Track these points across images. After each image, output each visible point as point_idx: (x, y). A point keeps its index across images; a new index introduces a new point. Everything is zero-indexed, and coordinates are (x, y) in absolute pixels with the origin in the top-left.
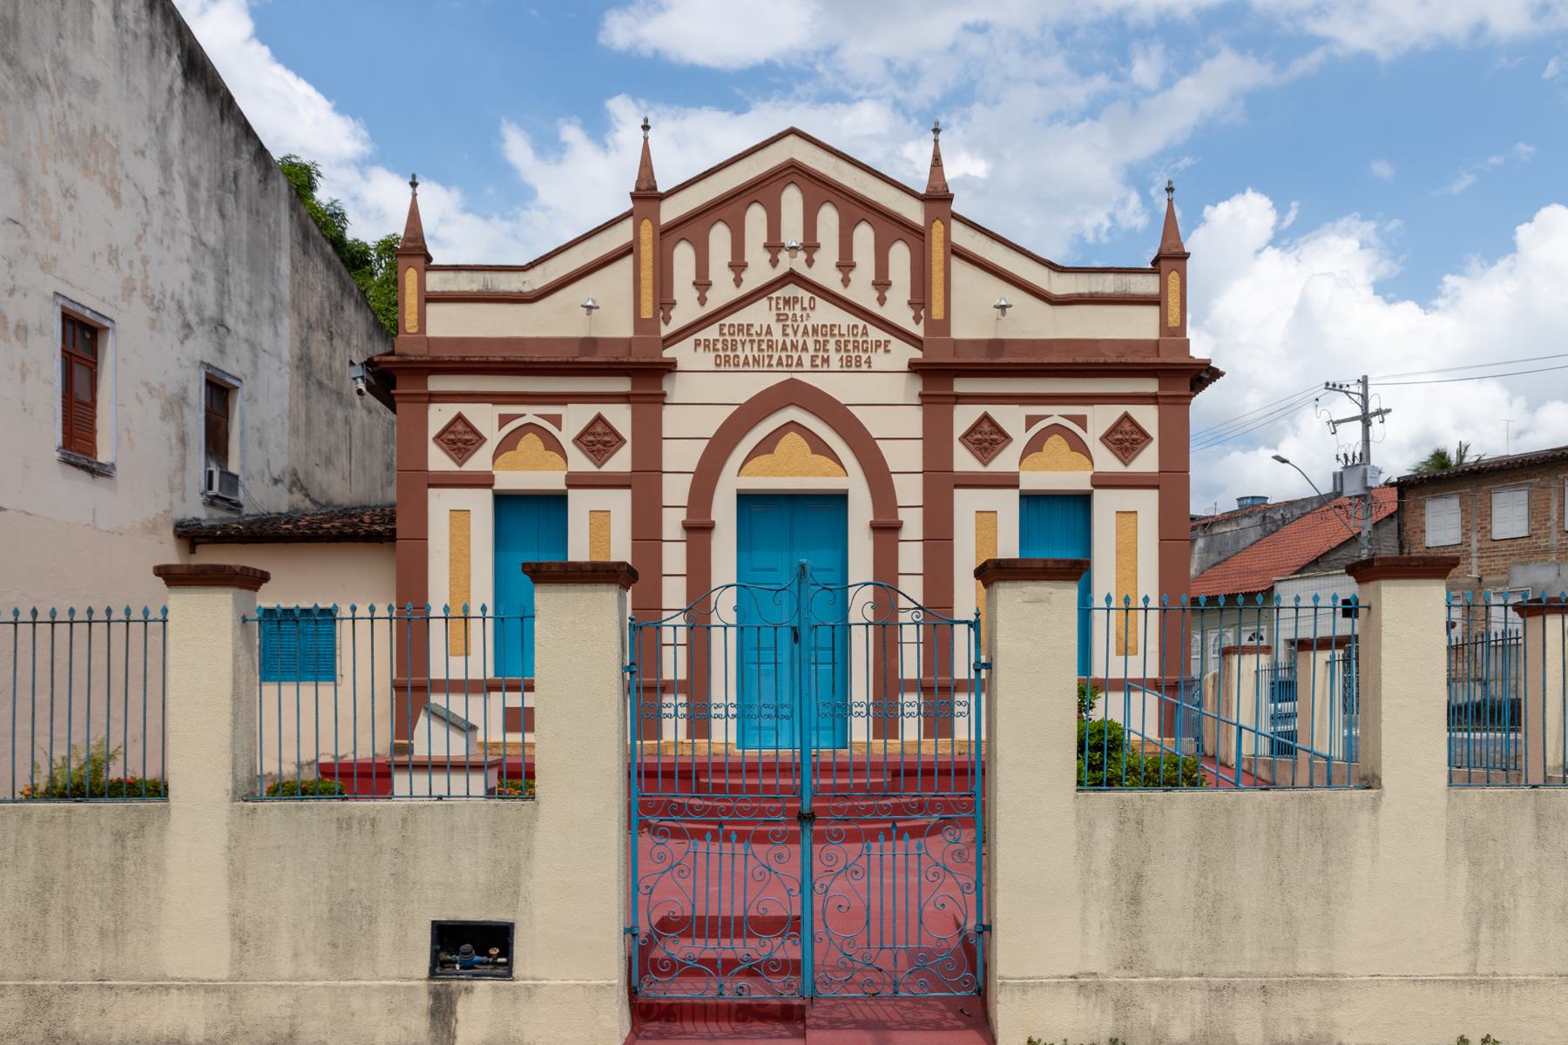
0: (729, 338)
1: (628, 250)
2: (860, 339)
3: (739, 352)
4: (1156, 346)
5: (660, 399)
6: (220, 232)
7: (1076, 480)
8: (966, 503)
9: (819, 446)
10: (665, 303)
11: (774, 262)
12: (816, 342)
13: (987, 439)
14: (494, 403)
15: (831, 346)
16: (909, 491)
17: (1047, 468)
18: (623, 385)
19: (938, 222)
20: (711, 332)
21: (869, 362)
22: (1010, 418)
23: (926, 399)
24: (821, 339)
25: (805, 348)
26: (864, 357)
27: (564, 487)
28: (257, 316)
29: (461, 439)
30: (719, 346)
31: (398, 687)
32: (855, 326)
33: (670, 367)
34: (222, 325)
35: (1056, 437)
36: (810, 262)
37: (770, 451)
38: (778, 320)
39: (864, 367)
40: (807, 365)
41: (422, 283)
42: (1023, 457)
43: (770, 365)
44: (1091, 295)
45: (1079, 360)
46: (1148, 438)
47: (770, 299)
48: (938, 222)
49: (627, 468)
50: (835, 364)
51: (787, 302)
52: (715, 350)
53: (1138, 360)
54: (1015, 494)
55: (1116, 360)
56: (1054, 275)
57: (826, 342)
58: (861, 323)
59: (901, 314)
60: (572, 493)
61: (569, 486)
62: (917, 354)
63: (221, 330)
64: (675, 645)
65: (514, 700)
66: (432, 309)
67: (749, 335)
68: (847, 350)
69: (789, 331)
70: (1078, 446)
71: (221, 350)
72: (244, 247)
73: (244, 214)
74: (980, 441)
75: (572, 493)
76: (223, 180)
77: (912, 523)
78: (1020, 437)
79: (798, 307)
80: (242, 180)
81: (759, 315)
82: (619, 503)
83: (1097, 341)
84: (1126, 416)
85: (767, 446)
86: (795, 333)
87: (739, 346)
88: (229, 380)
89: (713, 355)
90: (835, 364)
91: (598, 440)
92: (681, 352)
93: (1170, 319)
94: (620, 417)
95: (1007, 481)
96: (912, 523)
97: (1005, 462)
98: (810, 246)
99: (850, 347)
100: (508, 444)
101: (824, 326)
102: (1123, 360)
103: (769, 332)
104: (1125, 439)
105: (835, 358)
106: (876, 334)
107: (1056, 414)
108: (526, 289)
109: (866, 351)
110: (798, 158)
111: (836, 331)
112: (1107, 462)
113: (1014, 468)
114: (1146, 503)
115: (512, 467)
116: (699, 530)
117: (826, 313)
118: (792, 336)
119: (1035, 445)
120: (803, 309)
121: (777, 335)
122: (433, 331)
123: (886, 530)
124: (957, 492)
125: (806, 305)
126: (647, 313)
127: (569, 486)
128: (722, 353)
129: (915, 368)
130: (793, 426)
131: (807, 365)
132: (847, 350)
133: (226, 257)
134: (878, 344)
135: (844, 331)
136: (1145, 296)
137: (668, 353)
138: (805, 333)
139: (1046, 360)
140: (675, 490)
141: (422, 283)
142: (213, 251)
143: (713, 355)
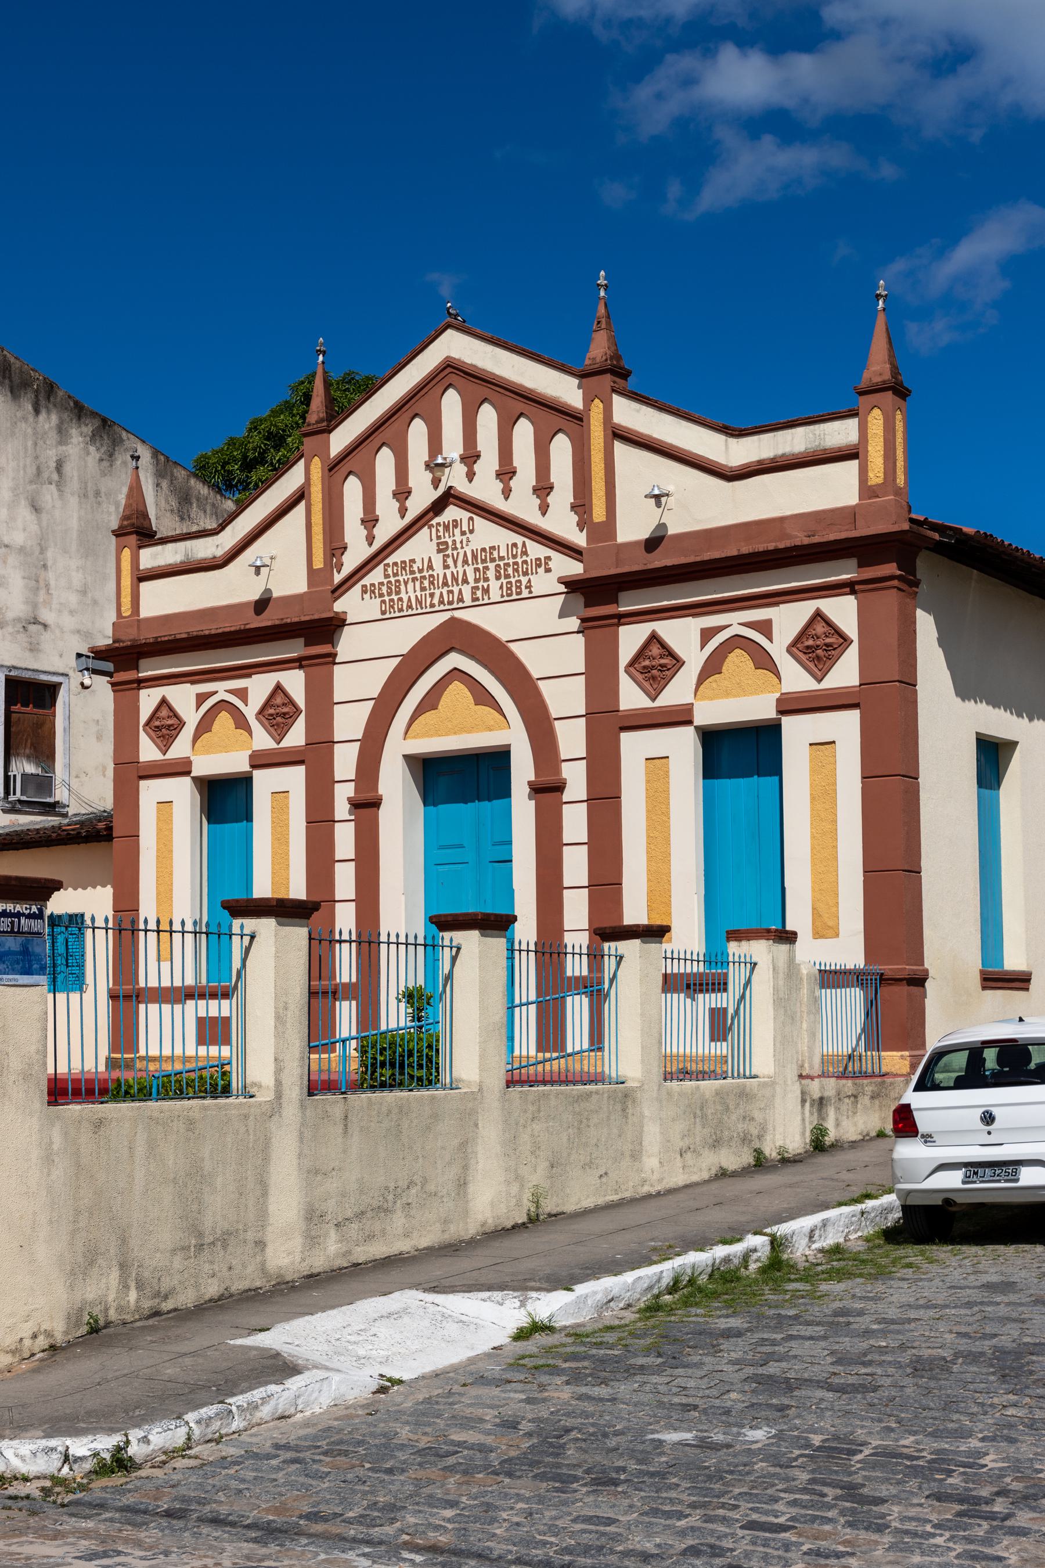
0: (393, 579)
1: (300, 496)
2: (519, 560)
3: (403, 595)
4: (849, 514)
5: (330, 659)
6: (34, 528)
7: (759, 707)
8: (635, 748)
9: (483, 697)
10: (336, 548)
11: (436, 483)
12: (477, 570)
13: (657, 665)
14: (193, 683)
15: (491, 574)
16: (572, 739)
17: (727, 694)
18: (295, 649)
19: (597, 401)
20: (376, 576)
21: (529, 587)
22: (682, 635)
23: (587, 626)
24: (480, 566)
25: (465, 581)
26: (524, 580)
27: (247, 768)
28: (95, 602)
29: (165, 726)
30: (384, 589)
31: (113, 996)
32: (515, 545)
33: (338, 623)
34: (36, 622)
35: (738, 651)
36: (471, 476)
37: (434, 707)
38: (439, 551)
39: (525, 593)
40: (468, 601)
41: (135, 560)
42: (701, 681)
43: (432, 605)
44: (773, 460)
45: (761, 547)
46: (846, 641)
47: (430, 527)
48: (597, 401)
49: (302, 742)
50: (495, 595)
51: (446, 527)
52: (381, 595)
53: (832, 537)
54: (689, 732)
55: (806, 541)
56: (732, 441)
57: (486, 568)
58: (519, 539)
59: (562, 523)
60: (257, 774)
61: (254, 766)
62: (575, 568)
63: (33, 628)
64: (350, 942)
65: (214, 1008)
66: (144, 586)
67: (412, 572)
68: (507, 576)
69: (450, 561)
70: (764, 661)
71: (34, 648)
72: (75, 535)
73: (73, 501)
74: (646, 670)
75: (257, 774)
76: (39, 472)
77: (576, 779)
78: (694, 657)
79: (457, 531)
80: (69, 469)
81: (420, 548)
82: (293, 780)
83: (782, 520)
84: (818, 615)
85: (430, 702)
86: (455, 562)
87: (403, 587)
88: (44, 677)
89: (379, 600)
90: (495, 595)
91: (278, 712)
92: (350, 604)
93: (871, 475)
94: (294, 682)
95: (679, 717)
96: (576, 779)
97: (678, 691)
98: (471, 457)
99: (510, 571)
100: (204, 726)
101: (484, 550)
102: (816, 539)
103: (430, 567)
104: (818, 646)
105: (494, 585)
106: (537, 550)
107: (734, 622)
108: (219, 553)
109: (525, 574)
110: (455, 355)
111: (495, 554)
112: (796, 678)
113: (687, 698)
114: (845, 728)
115: (208, 752)
116: (366, 805)
117: (488, 535)
118: (452, 568)
119: (712, 667)
120: (463, 533)
121: (438, 569)
122: (145, 613)
123: (548, 790)
124: (625, 737)
125: (465, 528)
126: (318, 563)
127: (254, 766)
128: (387, 598)
129: (572, 585)
130: (456, 673)
131: (468, 601)
132: (507, 576)
133: (42, 551)
134: (538, 562)
135: (503, 553)
136: (840, 449)
137: (338, 606)
138: (465, 562)
139: (707, 556)
140: (345, 762)
141: (135, 560)
142: (22, 550)
143: (379, 600)
